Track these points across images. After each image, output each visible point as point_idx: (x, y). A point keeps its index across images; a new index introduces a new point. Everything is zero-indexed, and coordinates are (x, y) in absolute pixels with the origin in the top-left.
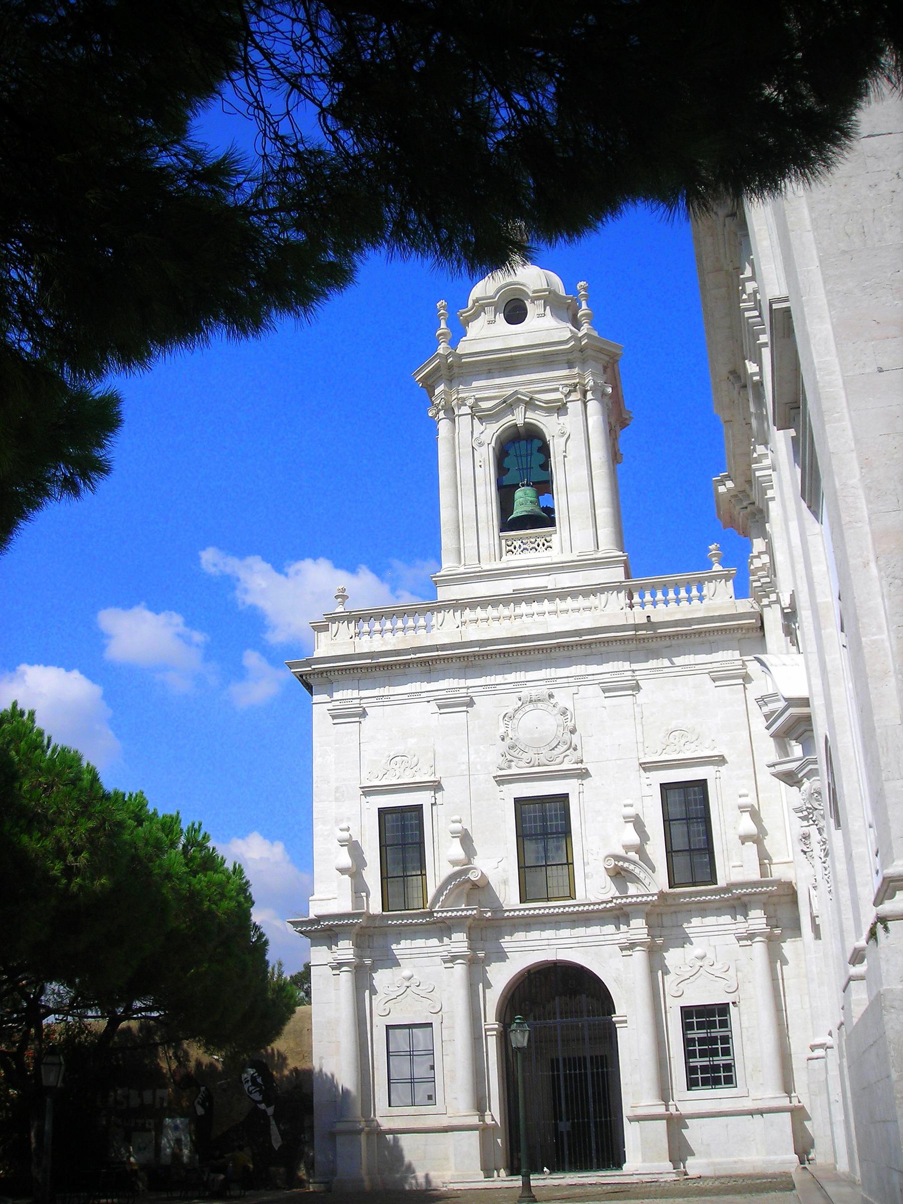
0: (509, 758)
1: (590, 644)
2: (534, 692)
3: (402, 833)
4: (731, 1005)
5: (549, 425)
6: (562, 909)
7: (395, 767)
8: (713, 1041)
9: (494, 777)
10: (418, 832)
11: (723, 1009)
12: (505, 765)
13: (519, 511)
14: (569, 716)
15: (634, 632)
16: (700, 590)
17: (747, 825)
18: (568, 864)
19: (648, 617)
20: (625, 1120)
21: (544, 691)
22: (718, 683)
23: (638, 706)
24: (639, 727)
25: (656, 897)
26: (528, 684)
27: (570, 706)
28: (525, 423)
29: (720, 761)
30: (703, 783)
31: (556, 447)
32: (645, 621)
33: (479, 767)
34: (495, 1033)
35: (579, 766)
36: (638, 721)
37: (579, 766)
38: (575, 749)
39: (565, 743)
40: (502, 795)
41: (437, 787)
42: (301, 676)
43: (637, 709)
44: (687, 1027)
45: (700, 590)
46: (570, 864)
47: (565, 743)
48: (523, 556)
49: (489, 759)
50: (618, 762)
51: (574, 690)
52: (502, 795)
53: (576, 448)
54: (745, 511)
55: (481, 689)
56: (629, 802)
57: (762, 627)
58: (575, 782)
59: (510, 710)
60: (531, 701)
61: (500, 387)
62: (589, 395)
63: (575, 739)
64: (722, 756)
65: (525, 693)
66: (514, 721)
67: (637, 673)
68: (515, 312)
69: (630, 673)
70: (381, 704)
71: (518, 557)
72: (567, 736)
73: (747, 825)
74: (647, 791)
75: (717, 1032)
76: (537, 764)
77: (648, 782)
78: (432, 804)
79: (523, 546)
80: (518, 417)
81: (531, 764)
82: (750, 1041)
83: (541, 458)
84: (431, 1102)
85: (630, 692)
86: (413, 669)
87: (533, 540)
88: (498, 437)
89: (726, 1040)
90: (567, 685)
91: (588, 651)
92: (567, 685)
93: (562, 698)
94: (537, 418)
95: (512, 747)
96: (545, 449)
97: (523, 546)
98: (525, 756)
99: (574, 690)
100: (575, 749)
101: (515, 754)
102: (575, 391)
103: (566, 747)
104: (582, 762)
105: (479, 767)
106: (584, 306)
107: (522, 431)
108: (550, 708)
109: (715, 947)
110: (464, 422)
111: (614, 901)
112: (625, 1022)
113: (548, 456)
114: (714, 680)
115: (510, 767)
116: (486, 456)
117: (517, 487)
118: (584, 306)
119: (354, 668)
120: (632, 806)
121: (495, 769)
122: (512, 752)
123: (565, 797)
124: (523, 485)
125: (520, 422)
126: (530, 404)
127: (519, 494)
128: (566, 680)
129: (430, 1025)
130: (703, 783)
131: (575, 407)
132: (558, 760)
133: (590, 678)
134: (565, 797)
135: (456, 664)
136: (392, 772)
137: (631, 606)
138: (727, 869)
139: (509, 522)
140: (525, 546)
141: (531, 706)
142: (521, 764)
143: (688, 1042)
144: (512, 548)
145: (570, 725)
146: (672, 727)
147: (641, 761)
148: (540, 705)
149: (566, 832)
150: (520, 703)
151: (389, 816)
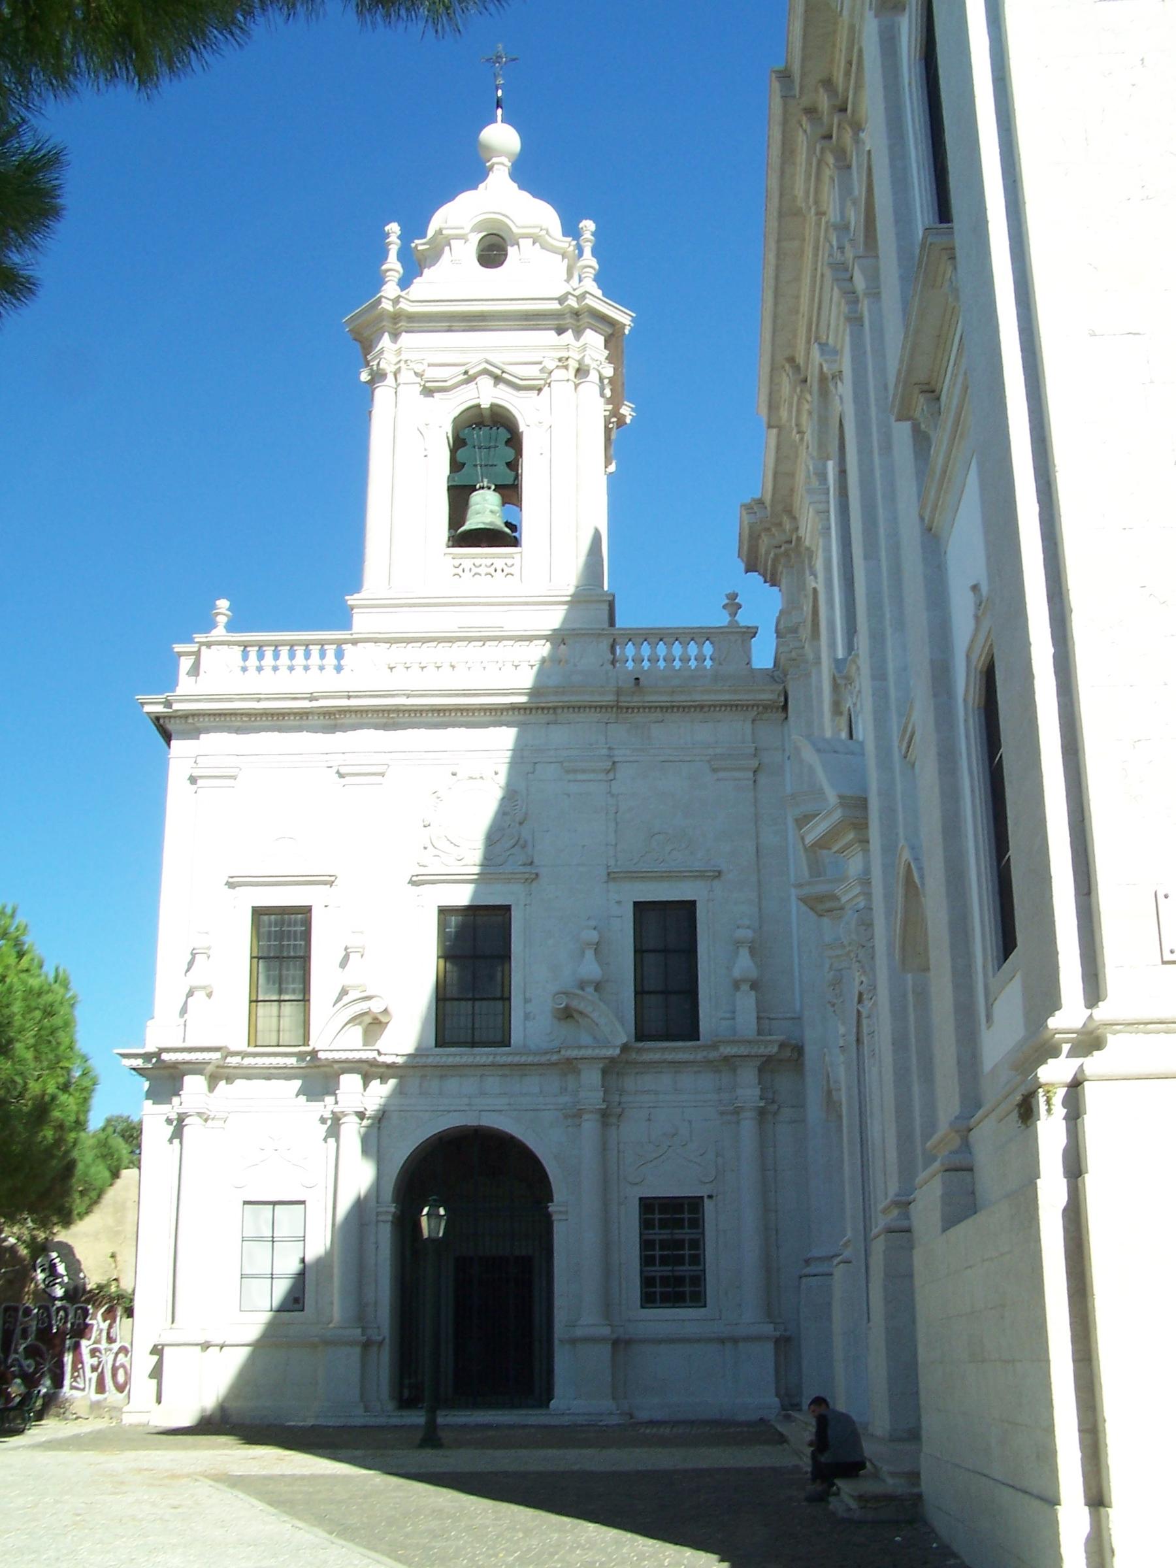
1: (555, 708)
3: (283, 945)
4: (706, 1200)
5: (525, 410)
6: (491, 1059)
8: (679, 1244)
11: (695, 1204)
13: (473, 522)
17: (744, 964)
18: (502, 999)
19: (637, 679)
20: (556, 1342)
22: (722, 774)
23: (613, 796)
25: (618, 1051)
30: (689, 907)
34: (390, 1218)
38: (524, 847)
42: (158, 719)
44: (646, 1224)
54: (777, 551)
57: (785, 707)
61: (463, 350)
64: (720, 872)
68: (493, 252)
73: (744, 964)
75: (685, 1234)
79: (475, 570)
82: (731, 1248)
83: (510, 453)
84: (296, 1306)
86: (313, 721)
87: (489, 562)
89: (697, 1244)
91: (551, 717)
96: (514, 440)
97: (475, 570)
102: (566, 367)
103: (512, 842)
104: (531, 863)
109: (690, 1122)
110: (411, 392)
111: (563, 1052)
112: (566, 1212)
113: (519, 452)
117: (473, 489)
119: (233, 714)
127: (476, 497)
129: (303, 1202)
143: (646, 1244)
144: (459, 571)
149: (505, 956)
151: (266, 918)
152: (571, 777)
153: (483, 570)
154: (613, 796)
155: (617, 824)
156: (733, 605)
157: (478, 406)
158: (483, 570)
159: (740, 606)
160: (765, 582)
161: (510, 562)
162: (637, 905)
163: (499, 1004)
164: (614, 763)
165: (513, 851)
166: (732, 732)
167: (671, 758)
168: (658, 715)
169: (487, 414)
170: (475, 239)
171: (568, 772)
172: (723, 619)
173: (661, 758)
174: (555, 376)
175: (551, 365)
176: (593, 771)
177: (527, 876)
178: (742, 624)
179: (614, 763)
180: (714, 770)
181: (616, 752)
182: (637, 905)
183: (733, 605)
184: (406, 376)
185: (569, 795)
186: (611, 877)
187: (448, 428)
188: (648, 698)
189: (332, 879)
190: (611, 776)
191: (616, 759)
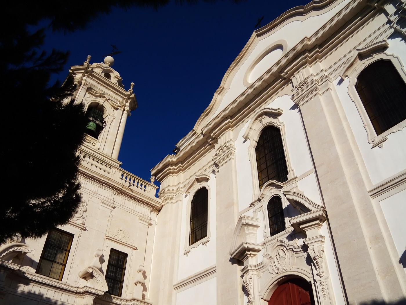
14: (85, 205)
15: (121, 188)
16: (145, 187)
18: (63, 265)
22: (141, 221)
23: (111, 215)
24: (110, 223)
25: (103, 293)
28: (102, 105)
35: (83, 225)
36: (110, 220)
45: (145, 187)
46: (64, 265)
50: (98, 232)
53: (115, 123)
57: (159, 211)
58: (78, 230)
62: (125, 112)
74: (105, 248)
77: (106, 245)
85: (110, 208)
88: (92, 103)
94: (107, 106)
104: (84, 224)
106: (131, 88)
118: (131, 88)
125: (101, 103)
127: (91, 123)
128: (89, 191)
130: (126, 255)
131: (120, 111)
134: (72, 236)
137: (122, 179)
138: (126, 293)
146: (121, 229)
154: (111, 215)
161: (95, 143)
162: (112, 249)
163: (61, 266)
166: (145, 210)
167: (129, 211)
173: (127, 210)
177: (83, 227)
181: (115, 203)
182: (112, 249)
186: (108, 238)
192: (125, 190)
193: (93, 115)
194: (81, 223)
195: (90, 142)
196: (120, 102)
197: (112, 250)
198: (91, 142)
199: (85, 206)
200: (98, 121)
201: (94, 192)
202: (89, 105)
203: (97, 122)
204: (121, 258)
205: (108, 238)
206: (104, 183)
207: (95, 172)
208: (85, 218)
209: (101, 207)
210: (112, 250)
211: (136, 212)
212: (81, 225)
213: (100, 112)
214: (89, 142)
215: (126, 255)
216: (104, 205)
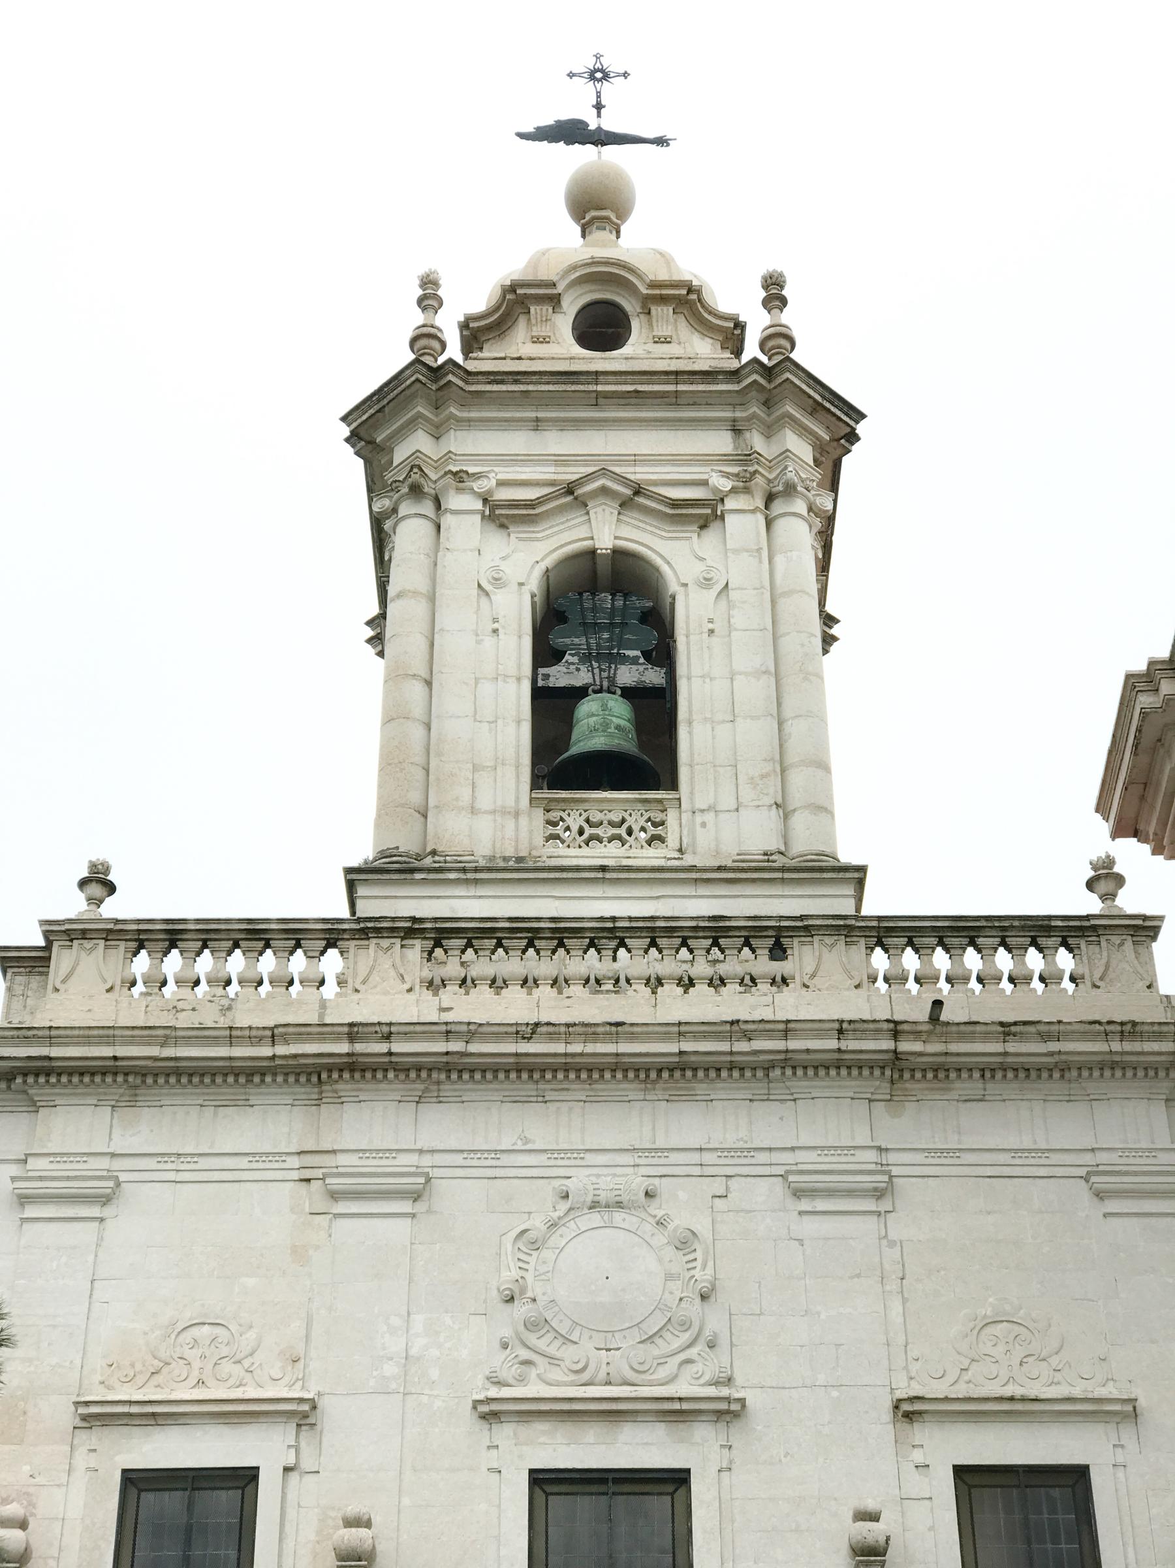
0: (525, 1354)
1: (768, 1068)
2: (607, 1184)
5: (680, 561)
7: (188, 1354)
9: (476, 1404)
10: (233, 1554)
12: (506, 1374)
15: (887, 1044)
21: (634, 1182)
22: (1113, 1206)
23: (892, 1244)
26: (591, 1159)
27: (702, 1226)
29: (1127, 1413)
31: (691, 614)
32: (922, 1014)
33: (434, 1374)
36: (893, 1286)
37: (724, 1392)
38: (711, 1345)
39: (685, 1325)
40: (493, 1459)
41: (303, 1416)
43: (896, 1253)
47: (685, 1325)
48: (585, 851)
49: (470, 1351)
50: (835, 1394)
51: (718, 1186)
52: (493, 1459)
55: (458, 1159)
56: (871, 1505)
59: (537, 1223)
60: (594, 1205)
63: (715, 1322)
64: (1133, 1401)
65: (580, 1181)
66: (547, 1254)
67: (892, 1158)
69: (872, 1156)
70: (171, 1176)
71: (573, 852)
72: (694, 1308)
74: (916, 1484)
76: (602, 1375)
77: (918, 1456)
78: (287, 1470)
80: (606, 531)
81: (585, 1376)
85: (869, 1205)
87: (616, 817)
90: (697, 1171)
92: (697, 1171)
93: (684, 1205)
95: (531, 1325)
97: (588, 831)
98: (569, 1354)
99: (718, 1186)
100: (711, 1345)
101: (541, 1344)
102: (747, 490)
103: (686, 1337)
104: (729, 1381)
105: (434, 1374)
107: (603, 568)
108: (648, 1228)
114: (1100, 1195)
115: (522, 1380)
116: (516, 612)
120: (874, 1517)
121: (480, 1381)
122: (532, 1339)
123: (679, 1479)
124: (600, 691)
126: (633, 498)
127: (587, 709)
128: (695, 1157)
130: (1078, 1476)
132: (662, 1373)
133: (763, 1157)
135: (394, 1089)
136: (178, 1368)
139: (561, 767)
140: (599, 831)
141: (595, 1219)
142: (555, 1374)
145: (703, 1276)
147: (899, 1394)
148: (618, 1217)
150: (563, 1206)
152: (805, 1205)
153: (605, 832)
154: (892, 1244)
155: (905, 1301)
156: (1105, 878)
157: (592, 553)
158: (605, 832)
159: (1120, 880)
160: (1155, 852)
161: (658, 817)
164: (891, 1177)
165: (693, 1352)
167: (1007, 1171)
168: (974, 1086)
169: (603, 568)
170: (572, 305)
171: (798, 1193)
172: (1091, 905)
173: (989, 1171)
174: (730, 504)
175: (726, 485)
176: (850, 1193)
177: (723, 1406)
178: (1130, 911)
179: (891, 1177)
180: (1100, 1195)
183: (1105, 878)
184: (455, 501)
185: (801, 1242)
187: (534, 584)
188: (954, 1048)
189: (306, 1407)
190: (885, 1205)
191: (895, 1171)
192: (917, 1047)
193: (588, 644)
194: (707, 1378)
195: (622, 831)
196: (725, 459)
197: (961, 1472)
198: (625, 826)
199: (698, 1264)
200: (634, 661)
201: (729, 1150)
202: (533, 596)
203: (627, 676)
204: (1053, 1511)
205: (908, 1412)
206: (768, 1068)
207: (683, 1028)
208: (724, 1341)
209: (810, 1226)
210: (961, 1472)
211: (1055, 1158)
212: (712, 1391)
213: (626, 596)
214: (616, 831)
215: (1078, 1476)
216: (821, 1205)
